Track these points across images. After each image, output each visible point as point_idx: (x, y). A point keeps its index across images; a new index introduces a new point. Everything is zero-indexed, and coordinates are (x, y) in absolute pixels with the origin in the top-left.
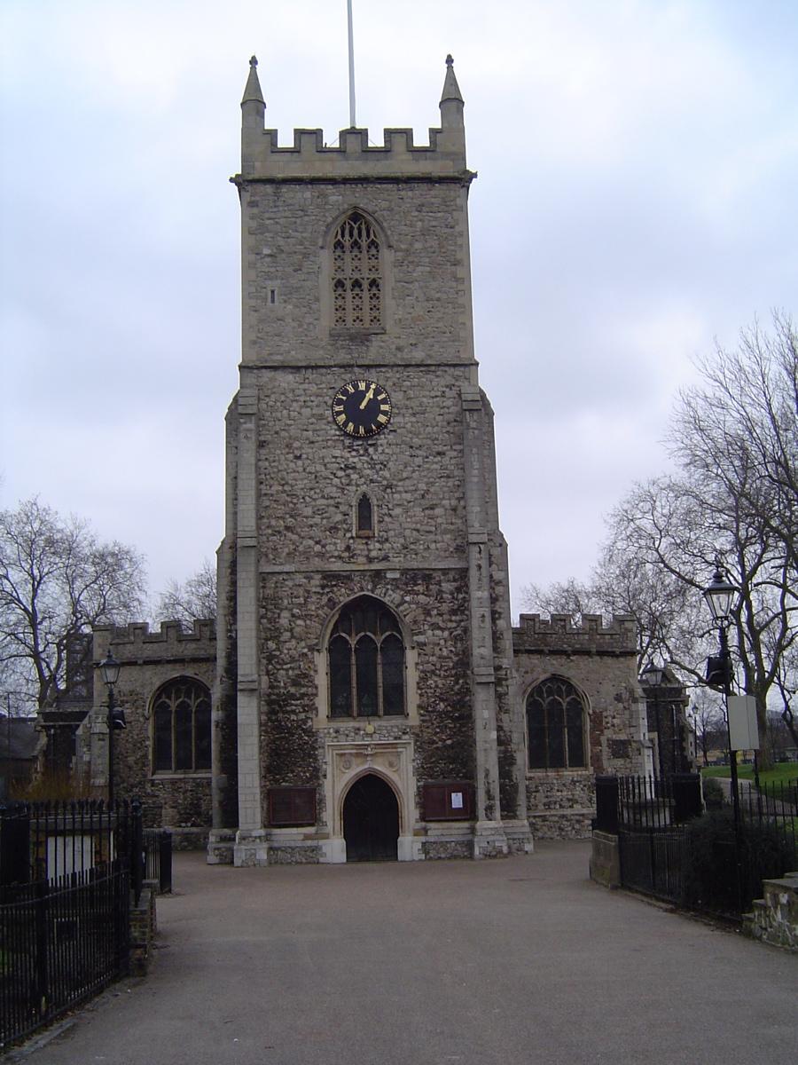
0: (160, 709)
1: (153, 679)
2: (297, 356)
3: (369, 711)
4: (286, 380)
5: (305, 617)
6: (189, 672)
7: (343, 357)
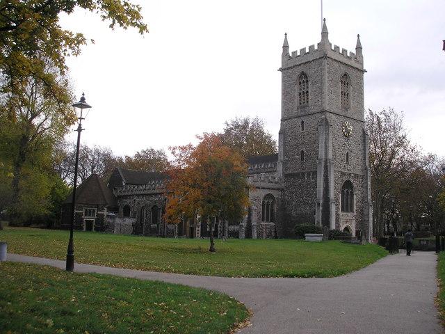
0: (264, 202)
1: (262, 193)
2: (336, 111)
3: (347, 211)
4: (334, 117)
5: (337, 184)
6: (271, 192)
7: (343, 114)
